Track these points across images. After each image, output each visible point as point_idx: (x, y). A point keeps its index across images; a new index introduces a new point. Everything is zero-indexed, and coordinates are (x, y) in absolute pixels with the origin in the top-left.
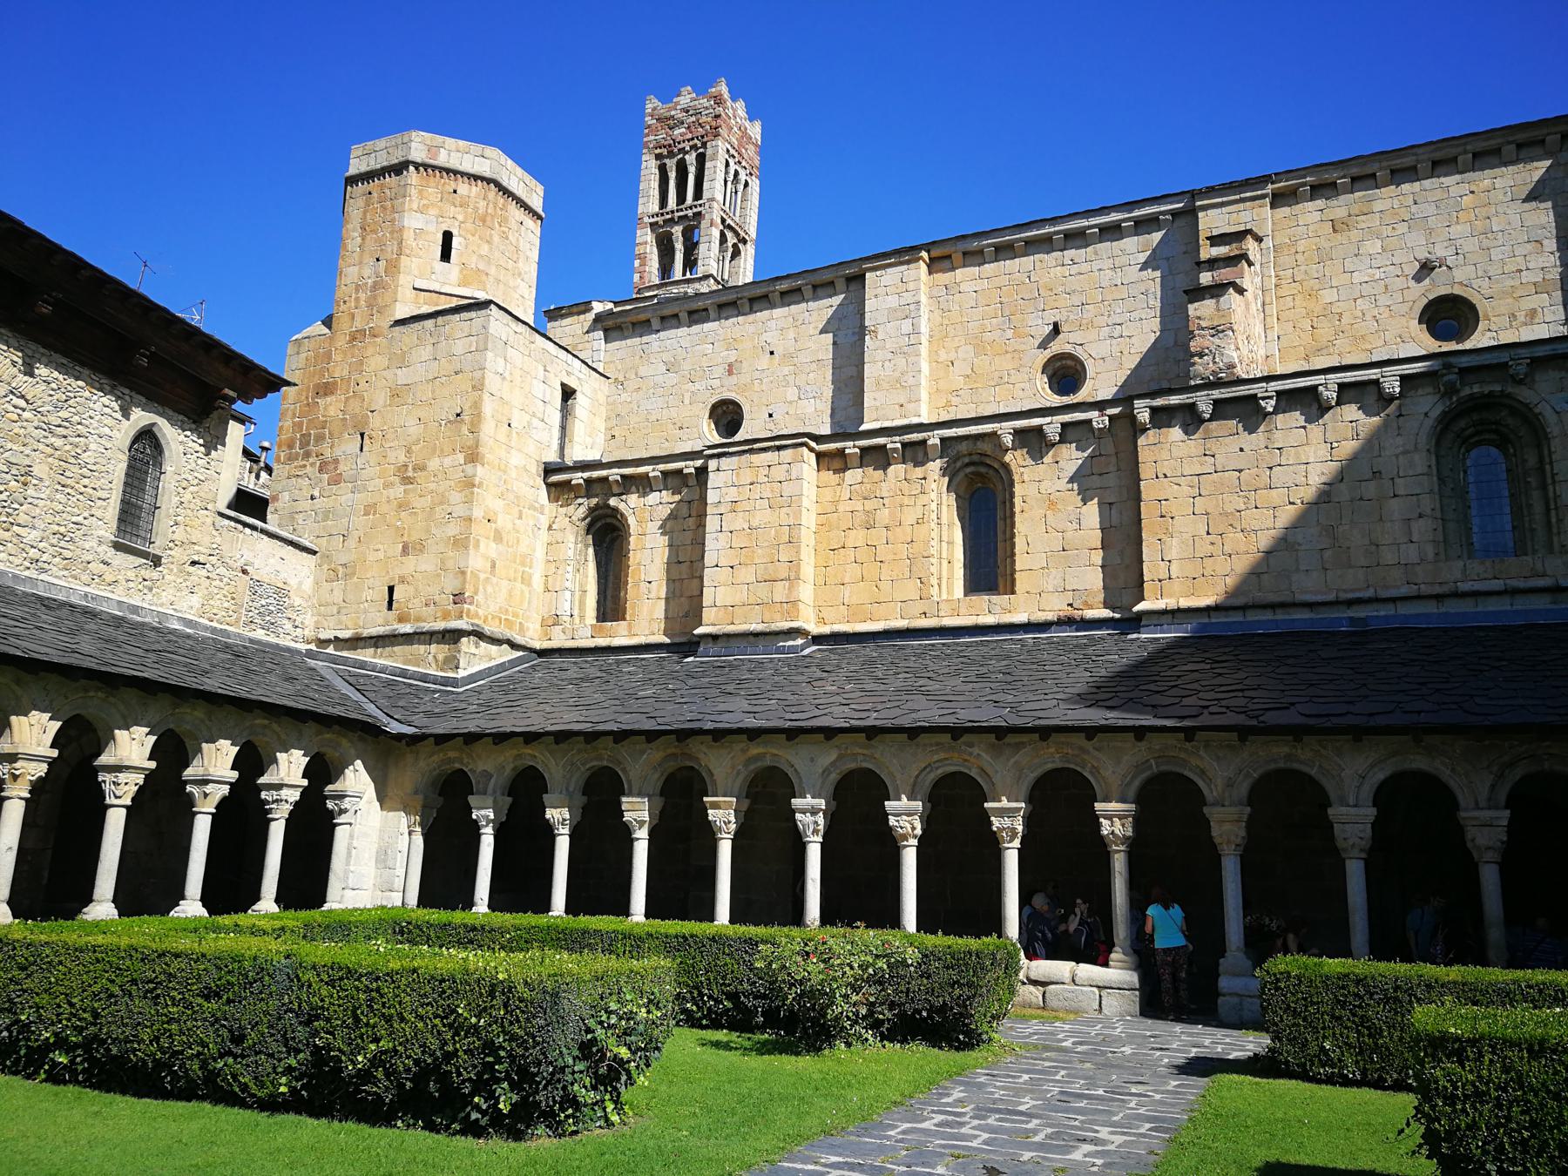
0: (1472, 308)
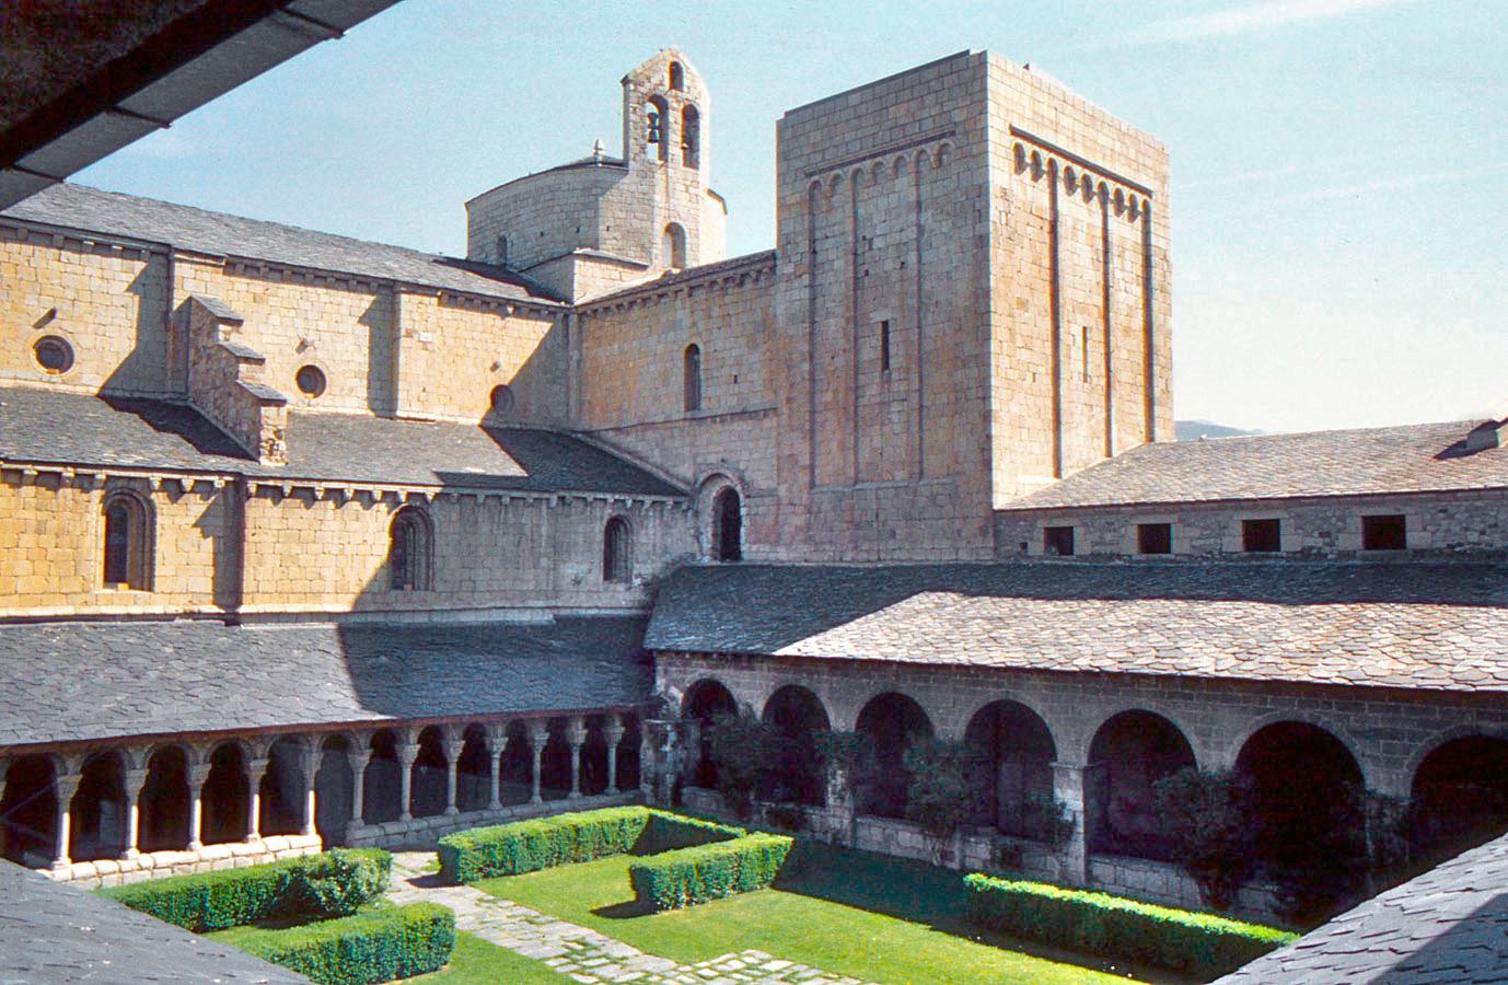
0: (321, 374)
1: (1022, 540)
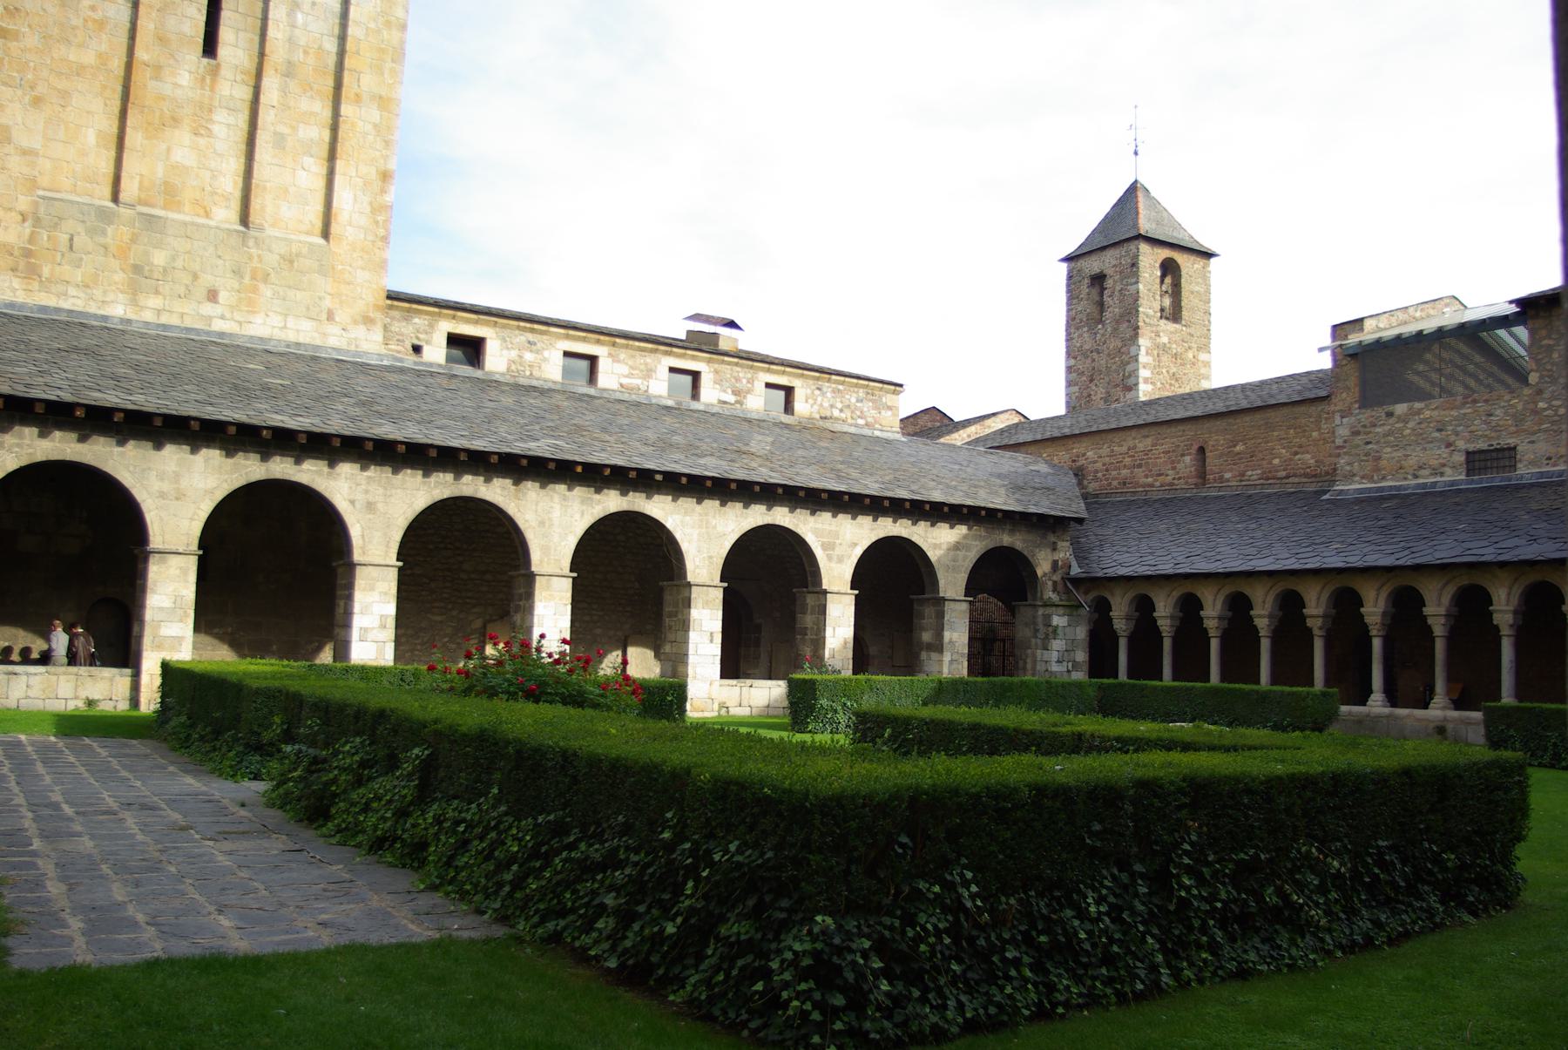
1: (417, 342)
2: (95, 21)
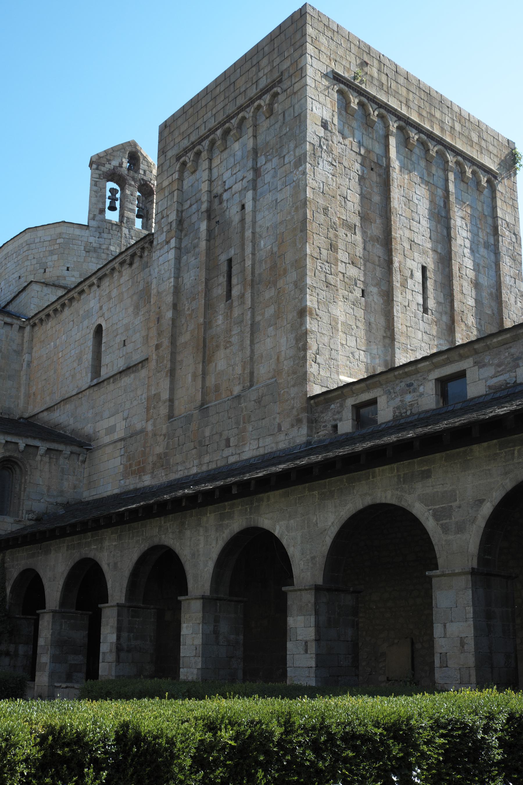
1: (333, 423)
2: (189, 315)
